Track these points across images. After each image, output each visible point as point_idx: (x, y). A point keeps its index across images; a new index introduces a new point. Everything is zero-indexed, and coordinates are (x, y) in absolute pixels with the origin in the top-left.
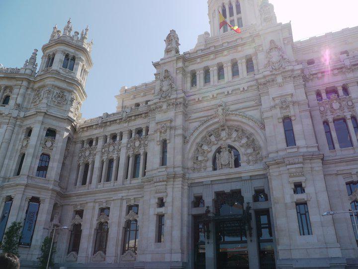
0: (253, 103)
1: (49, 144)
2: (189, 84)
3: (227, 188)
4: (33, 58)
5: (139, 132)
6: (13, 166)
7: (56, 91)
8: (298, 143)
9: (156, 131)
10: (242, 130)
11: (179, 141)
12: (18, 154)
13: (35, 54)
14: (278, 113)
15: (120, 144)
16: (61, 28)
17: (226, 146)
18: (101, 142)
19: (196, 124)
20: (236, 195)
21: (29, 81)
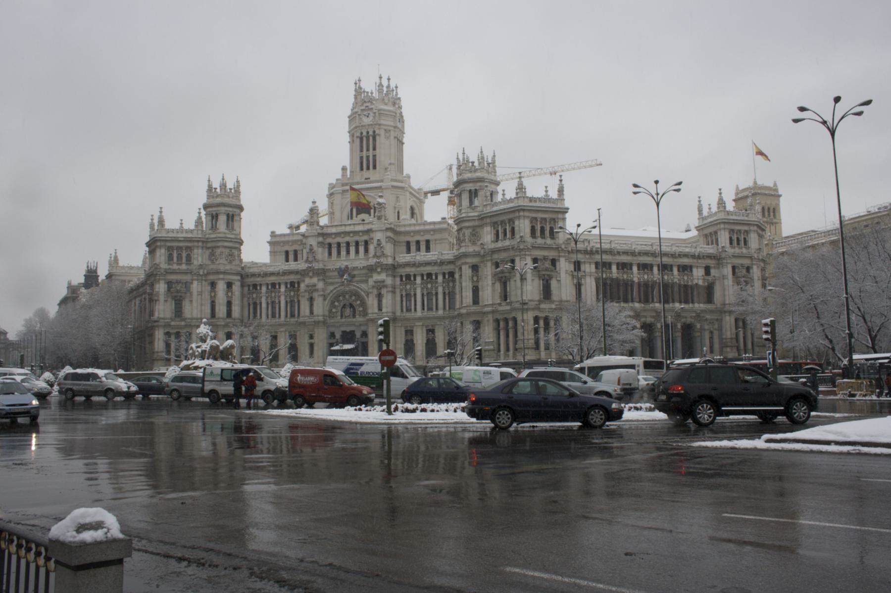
0: (364, 278)
1: (230, 294)
2: (326, 254)
3: (348, 329)
4: (200, 218)
5: (292, 284)
6: (208, 310)
7: (227, 251)
8: (384, 310)
9: (306, 291)
10: (358, 296)
11: (321, 299)
12: (209, 301)
13: (200, 213)
14: (375, 292)
15: (279, 292)
16: (216, 184)
17: (348, 304)
18: (264, 289)
19: (331, 288)
20: (352, 333)
21: (203, 242)
